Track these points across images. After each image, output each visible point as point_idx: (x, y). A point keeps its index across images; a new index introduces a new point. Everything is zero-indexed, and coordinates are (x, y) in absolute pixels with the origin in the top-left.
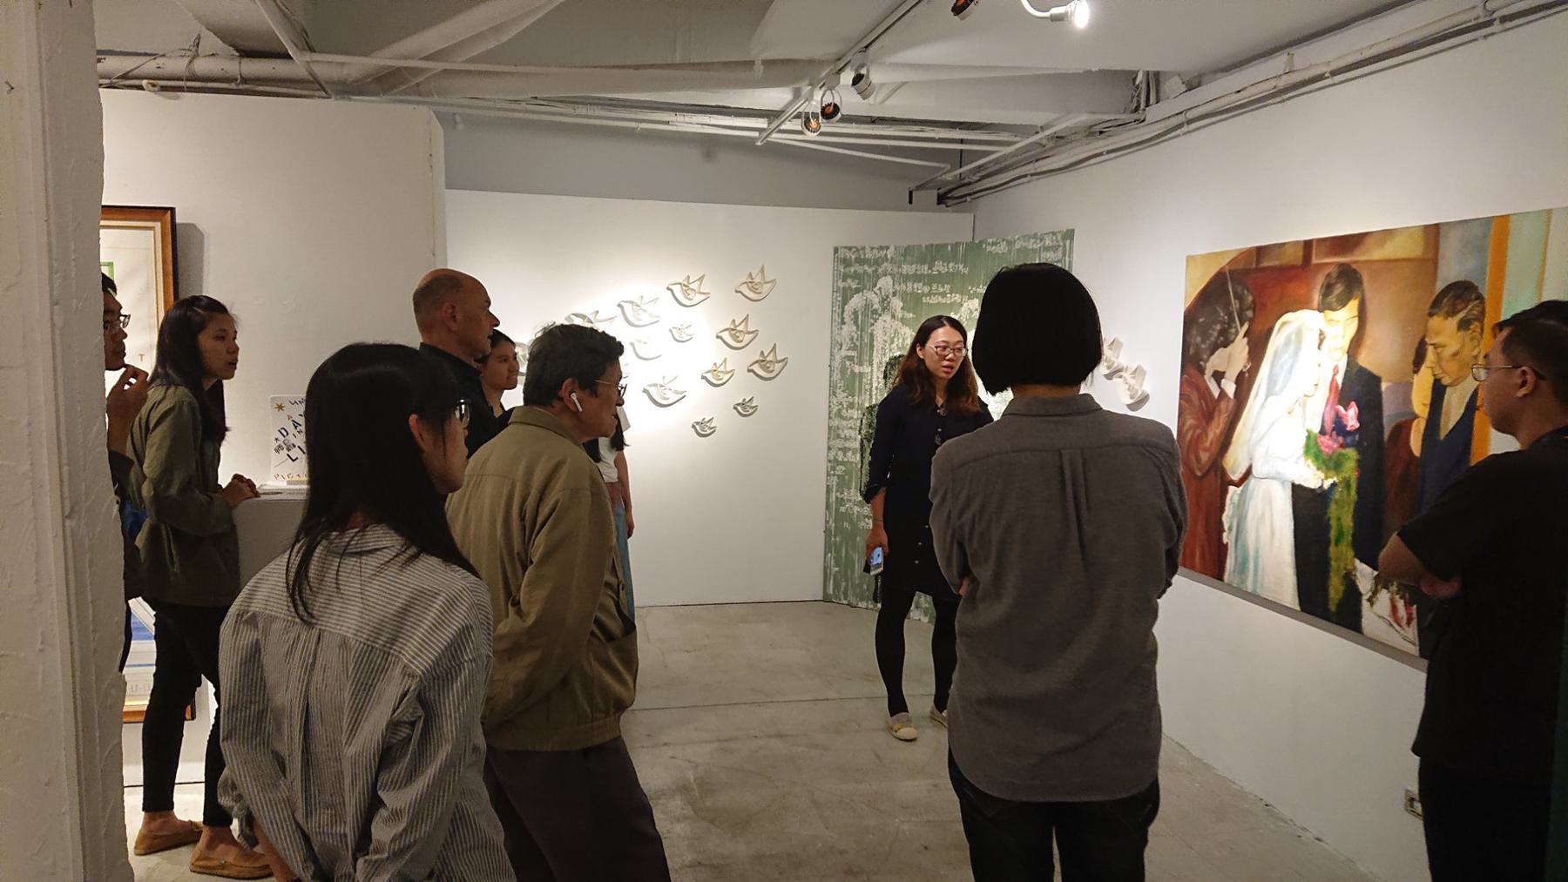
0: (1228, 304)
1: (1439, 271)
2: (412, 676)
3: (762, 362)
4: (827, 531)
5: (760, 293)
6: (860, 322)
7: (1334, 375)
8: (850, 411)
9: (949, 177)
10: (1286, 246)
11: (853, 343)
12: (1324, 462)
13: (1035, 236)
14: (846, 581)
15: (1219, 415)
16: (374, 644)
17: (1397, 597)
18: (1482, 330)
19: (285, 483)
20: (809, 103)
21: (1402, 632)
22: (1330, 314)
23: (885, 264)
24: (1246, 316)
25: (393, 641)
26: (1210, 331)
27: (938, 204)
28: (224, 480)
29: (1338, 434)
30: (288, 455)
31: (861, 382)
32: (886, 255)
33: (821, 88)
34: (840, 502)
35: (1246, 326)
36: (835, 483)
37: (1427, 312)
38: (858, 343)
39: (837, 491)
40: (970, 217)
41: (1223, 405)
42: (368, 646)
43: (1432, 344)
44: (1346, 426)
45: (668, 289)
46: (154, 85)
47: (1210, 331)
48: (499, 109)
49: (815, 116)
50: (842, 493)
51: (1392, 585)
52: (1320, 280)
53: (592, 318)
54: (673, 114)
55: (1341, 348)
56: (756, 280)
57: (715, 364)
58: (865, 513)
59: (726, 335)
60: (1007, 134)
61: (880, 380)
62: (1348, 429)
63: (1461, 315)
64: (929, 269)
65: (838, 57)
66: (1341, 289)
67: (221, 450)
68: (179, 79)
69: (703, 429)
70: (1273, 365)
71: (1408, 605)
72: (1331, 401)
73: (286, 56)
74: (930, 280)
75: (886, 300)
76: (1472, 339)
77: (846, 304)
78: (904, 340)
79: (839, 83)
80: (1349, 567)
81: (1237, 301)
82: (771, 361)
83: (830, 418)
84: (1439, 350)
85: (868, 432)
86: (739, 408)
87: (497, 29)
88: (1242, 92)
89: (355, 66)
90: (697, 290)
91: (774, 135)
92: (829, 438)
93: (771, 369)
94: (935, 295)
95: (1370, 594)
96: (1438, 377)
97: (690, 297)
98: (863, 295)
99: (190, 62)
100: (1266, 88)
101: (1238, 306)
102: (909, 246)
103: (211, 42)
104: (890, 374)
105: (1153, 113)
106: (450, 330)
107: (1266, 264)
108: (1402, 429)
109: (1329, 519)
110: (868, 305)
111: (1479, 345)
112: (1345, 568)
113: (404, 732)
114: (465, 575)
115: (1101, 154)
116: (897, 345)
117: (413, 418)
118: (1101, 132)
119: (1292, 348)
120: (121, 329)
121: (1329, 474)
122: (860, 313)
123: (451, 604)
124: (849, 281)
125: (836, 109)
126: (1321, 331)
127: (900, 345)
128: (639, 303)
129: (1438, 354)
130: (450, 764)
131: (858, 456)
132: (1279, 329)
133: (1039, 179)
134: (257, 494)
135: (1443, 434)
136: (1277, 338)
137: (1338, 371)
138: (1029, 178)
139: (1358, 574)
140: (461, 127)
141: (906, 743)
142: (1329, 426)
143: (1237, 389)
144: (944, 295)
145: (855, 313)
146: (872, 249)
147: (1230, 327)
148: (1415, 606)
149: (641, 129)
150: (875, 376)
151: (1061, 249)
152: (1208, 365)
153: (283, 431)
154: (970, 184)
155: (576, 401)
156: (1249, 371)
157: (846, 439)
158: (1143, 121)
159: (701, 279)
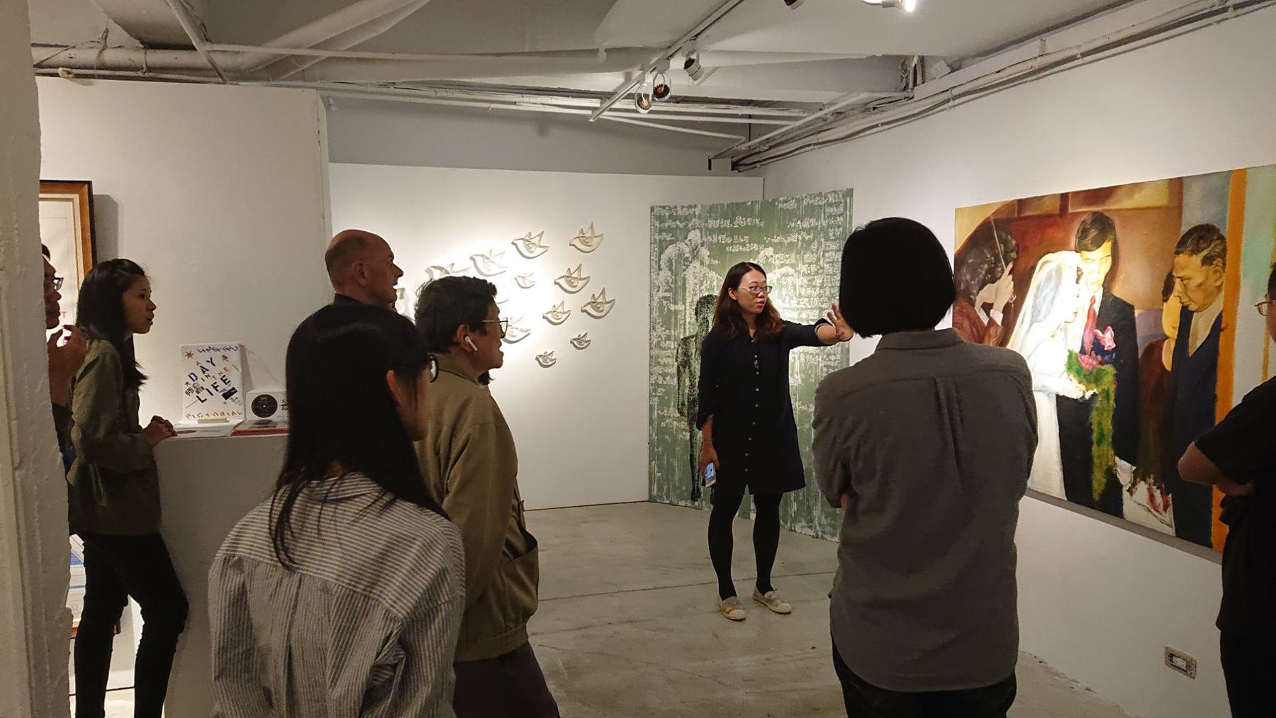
0: (994, 247)
1: (1183, 215)
2: (394, 620)
3: (593, 303)
4: (651, 443)
5: (590, 246)
6: (674, 268)
7: (1092, 305)
8: (668, 342)
9: (743, 147)
10: (1045, 198)
11: (668, 286)
12: (1085, 376)
13: (820, 195)
14: (668, 484)
15: (989, 339)
16: (355, 589)
17: (1155, 487)
18: (1224, 264)
19: (197, 422)
20: (641, 84)
21: (1159, 516)
22: (1086, 254)
23: (694, 220)
24: (1011, 258)
25: (373, 584)
26: (979, 270)
27: (733, 169)
28: (144, 422)
29: (1097, 354)
30: (197, 397)
31: (676, 319)
32: (694, 212)
33: (651, 72)
34: (661, 418)
35: (1011, 266)
36: (656, 403)
37: (1174, 250)
38: (673, 286)
39: (658, 410)
40: (758, 181)
41: (992, 330)
42: (350, 590)
43: (1178, 278)
44: (1104, 347)
45: (513, 243)
46: (69, 73)
47: (979, 270)
48: (372, 93)
49: (647, 96)
50: (663, 411)
51: (1150, 478)
52: (1076, 226)
53: (448, 269)
54: (520, 96)
55: (1097, 282)
57: (554, 306)
58: (683, 427)
59: (563, 282)
60: (798, 110)
62: (1106, 349)
63: (1205, 253)
64: (730, 223)
65: (668, 45)
66: (1095, 233)
67: (140, 394)
68: (92, 68)
69: (545, 361)
70: (1036, 297)
71: (1164, 494)
72: (1090, 326)
73: (190, 48)
74: (732, 232)
75: (695, 250)
76: (1215, 272)
77: (662, 253)
78: (711, 283)
79: (669, 67)
80: (1110, 463)
81: (1002, 245)
82: (601, 303)
83: (651, 349)
84: (1186, 282)
86: (575, 342)
87: (374, 23)
88: (1000, 73)
89: (250, 54)
90: (537, 244)
91: (606, 113)
92: (650, 366)
93: (600, 309)
94: (736, 244)
95: (1130, 485)
96: (1185, 305)
97: (532, 250)
98: (676, 246)
99: (100, 52)
100: (1024, 68)
101: (1002, 248)
102: (713, 205)
103: (119, 35)
105: (921, 91)
106: (359, 285)
107: (1028, 213)
108: (1154, 348)
109: (1091, 424)
110: (680, 255)
111: (1221, 277)
112: (1107, 464)
113: (387, 674)
114: (438, 520)
115: (876, 126)
116: (706, 287)
117: (390, 373)
118: (874, 108)
119: (1052, 283)
120: (55, 291)
121: (1090, 387)
122: (673, 261)
123: (428, 547)
124: (664, 234)
125: (667, 89)
126: (1078, 268)
128: (489, 257)
129: (1185, 285)
130: (431, 703)
131: (676, 380)
132: (1039, 271)
133: (819, 148)
134: (174, 434)
135: (1191, 352)
136: (1040, 273)
137: (1095, 302)
138: (812, 147)
139: (1119, 470)
140: (334, 108)
141: (734, 622)
142: (1088, 347)
143: (1004, 317)
144: (743, 245)
145: (670, 260)
146: (683, 207)
147: (996, 266)
148: (1171, 495)
149: (493, 109)
150: (688, 313)
151: (842, 205)
152: (977, 298)
153: (192, 376)
154: (760, 152)
155: (471, 343)
156: (1014, 302)
157: (665, 366)
158: (913, 98)
159: (541, 235)
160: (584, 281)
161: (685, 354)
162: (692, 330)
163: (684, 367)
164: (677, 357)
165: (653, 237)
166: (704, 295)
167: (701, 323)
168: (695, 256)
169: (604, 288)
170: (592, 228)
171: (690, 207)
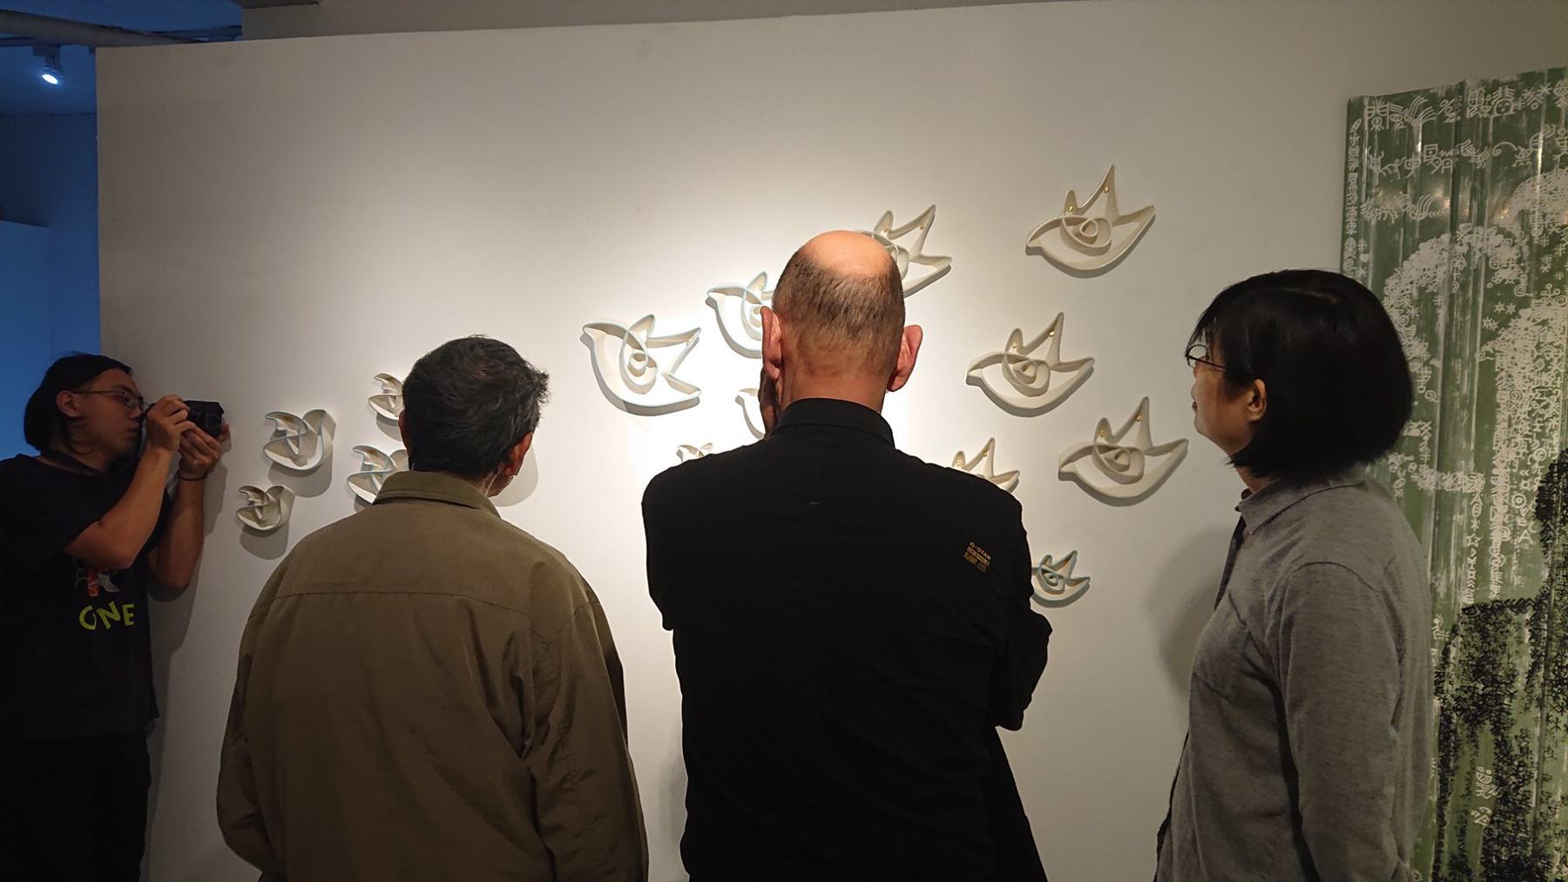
3: (1105, 451)
5: (1103, 251)
31: (1442, 524)
32: (1550, 99)
56: (1090, 215)
61: (1520, 521)
75: (1549, 249)
77: (1389, 273)
82: (1132, 450)
93: (1129, 473)
98: (1453, 241)
145: (1425, 300)
146: (1491, 88)
159: (924, 221)
161: (1481, 668)
162: (1517, 580)
163: (1473, 721)
164: (1441, 677)
165: (1353, 212)
169: (1146, 399)
170: (1108, 184)
171: (1531, 80)
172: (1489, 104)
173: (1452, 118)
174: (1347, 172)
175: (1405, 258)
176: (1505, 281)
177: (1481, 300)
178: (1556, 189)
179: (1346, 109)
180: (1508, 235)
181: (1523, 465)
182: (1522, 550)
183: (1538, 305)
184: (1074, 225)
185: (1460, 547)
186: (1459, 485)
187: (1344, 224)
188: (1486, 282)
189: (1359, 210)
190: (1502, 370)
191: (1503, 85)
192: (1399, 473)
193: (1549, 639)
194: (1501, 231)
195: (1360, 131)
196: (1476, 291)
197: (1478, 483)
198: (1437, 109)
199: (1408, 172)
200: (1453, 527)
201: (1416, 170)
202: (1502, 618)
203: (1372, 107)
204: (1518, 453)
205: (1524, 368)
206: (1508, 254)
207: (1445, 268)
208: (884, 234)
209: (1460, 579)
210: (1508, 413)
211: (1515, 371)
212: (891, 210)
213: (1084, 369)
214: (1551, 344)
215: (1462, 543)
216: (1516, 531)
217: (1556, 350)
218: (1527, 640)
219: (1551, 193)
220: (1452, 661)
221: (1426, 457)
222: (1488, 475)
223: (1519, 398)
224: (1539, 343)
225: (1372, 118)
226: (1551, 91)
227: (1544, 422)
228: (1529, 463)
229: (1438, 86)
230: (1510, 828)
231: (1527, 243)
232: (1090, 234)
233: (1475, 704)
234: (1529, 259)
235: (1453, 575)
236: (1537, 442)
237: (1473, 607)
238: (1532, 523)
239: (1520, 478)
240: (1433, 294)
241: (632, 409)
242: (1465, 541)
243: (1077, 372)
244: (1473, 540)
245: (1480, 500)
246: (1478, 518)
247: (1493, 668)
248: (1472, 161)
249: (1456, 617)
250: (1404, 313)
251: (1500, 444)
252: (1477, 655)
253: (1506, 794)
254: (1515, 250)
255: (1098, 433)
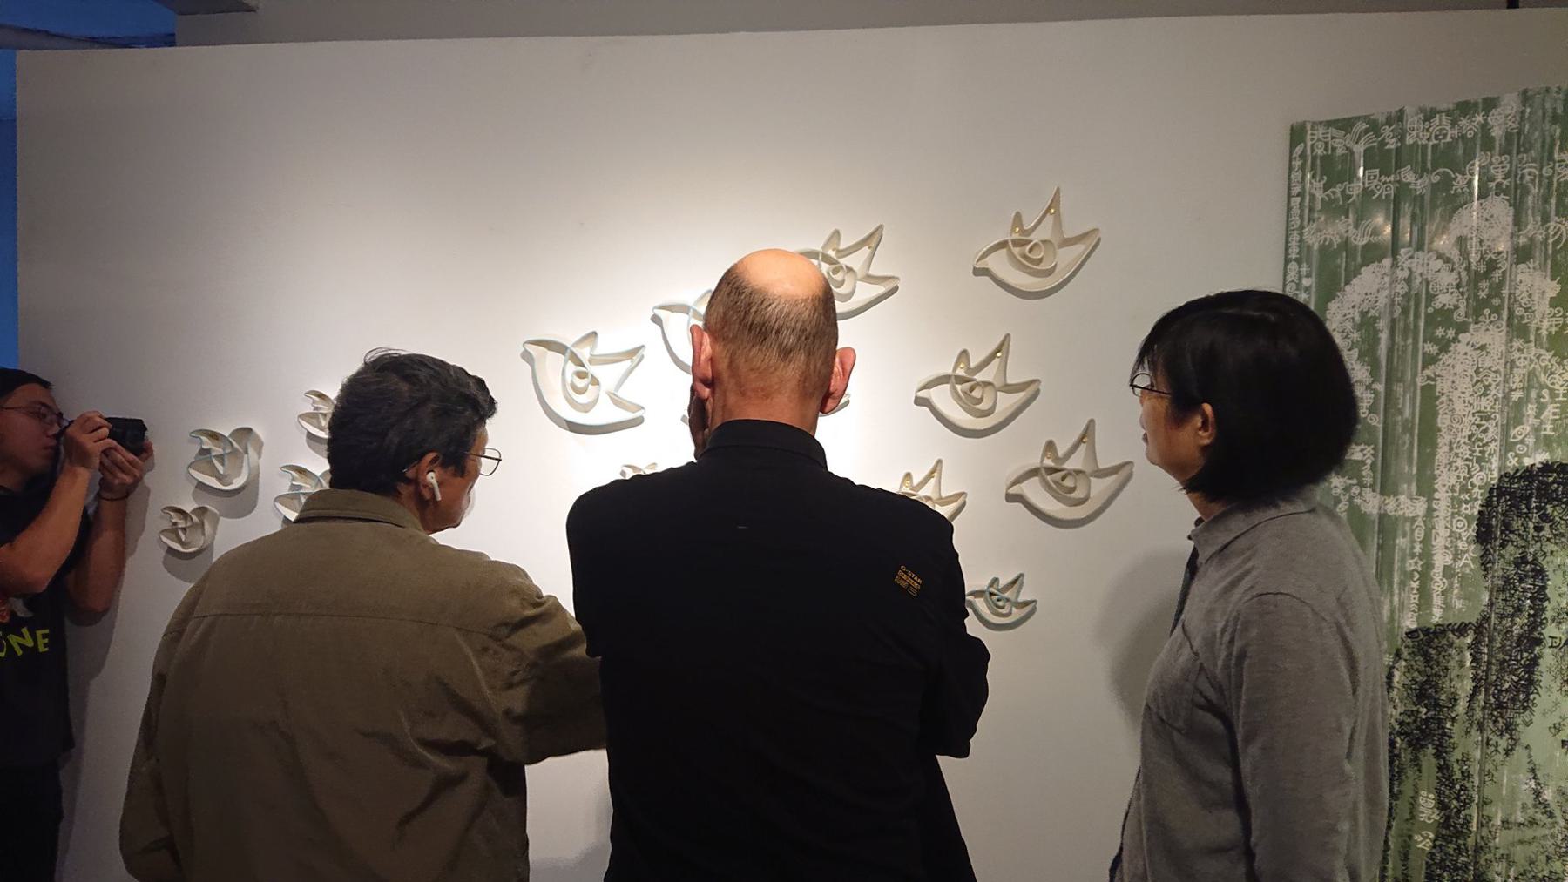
3: (1052, 473)
31: (1385, 548)
32: (1485, 127)
56: (1036, 237)
61: (1462, 545)
75: (1487, 275)
77: (1331, 297)
82: (1078, 472)
85: (1410, 713)
93: (1078, 494)
98: (1395, 265)
104: (1507, 526)
110: (1414, 299)
116: (1537, 430)
122: (1382, 324)
127: (1548, 430)
145: (1367, 323)
146: (1429, 115)
159: (872, 240)
160: (1022, 394)
161: (1425, 692)
163: (1416, 745)
165: (1295, 237)
166: (1527, 462)
167: (1507, 580)
168: (1485, 303)
169: (1092, 421)
171: (1466, 108)
172: (1428, 130)
173: (1392, 144)
174: (1289, 196)
175: (1347, 282)
176: (1444, 305)
177: (1422, 324)
178: (1492, 216)
179: (1289, 132)
180: (1448, 260)
181: (1464, 489)
182: (1463, 574)
183: (1477, 330)
184: (1020, 246)
185: (1403, 571)
186: (1401, 509)
187: (1287, 248)
188: (1427, 307)
189: (1301, 235)
190: (1443, 394)
191: (1440, 112)
192: (1342, 497)
193: (1489, 663)
194: (1440, 256)
195: (1303, 156)
196: (1417, 316)
197: (1420, 507)
198: (1378, 134)
199: (1350, 197)
200: (1397, 551)
201: (1358, 195)
202: (1444, 642)
203: (1315, 132)
204: (1459, 477)
205: (1463, 393)
206: (1447, 279)
207: (1387, 292)
208: (832, 253)
209: (1403, 603)
210: (1449, 437)
211: (1455, 395)
212: (838, 228)
213: (1030, 391)
214: (1490, 368)
215: (1405, 567)
216: (1457, 555)
217: (1493, 375)
218: (1468, 664)
219: (1487, 220)
220: (1395, 684)
221: (1369, 480)
222: (1430, 499)
223: (1460, 422)
224: (1478, 368)
225: (1315, 142)
226: (1486, 120)
227: (1484, 446)
228: (1469, 487)
229: (1379, 112)
230: (1452, 852)
231: (1466, 269)
232: (1035, 256)
233: (1418, 728)
234: (1468, 284)
235: (1396, 598)
236: (1477, 466)
237: (1416, 630)
238: (1473, 547)
239: (1460, 502)
240: (1375, 319)
241: (574, 428)
242: (1407, 565)
243: (1023, 394)
244: (1416, 563)
245: (1422, 524)
246: (1420, 542)
247: (1436, 692)
248: (1412, 187)
249: (1400, 642)
250: (1346, 337)
251: (1442, 468)
252: (1420, 679)
253: (1448, 818)
254: (1454, 275)
255: (1044, 455)
